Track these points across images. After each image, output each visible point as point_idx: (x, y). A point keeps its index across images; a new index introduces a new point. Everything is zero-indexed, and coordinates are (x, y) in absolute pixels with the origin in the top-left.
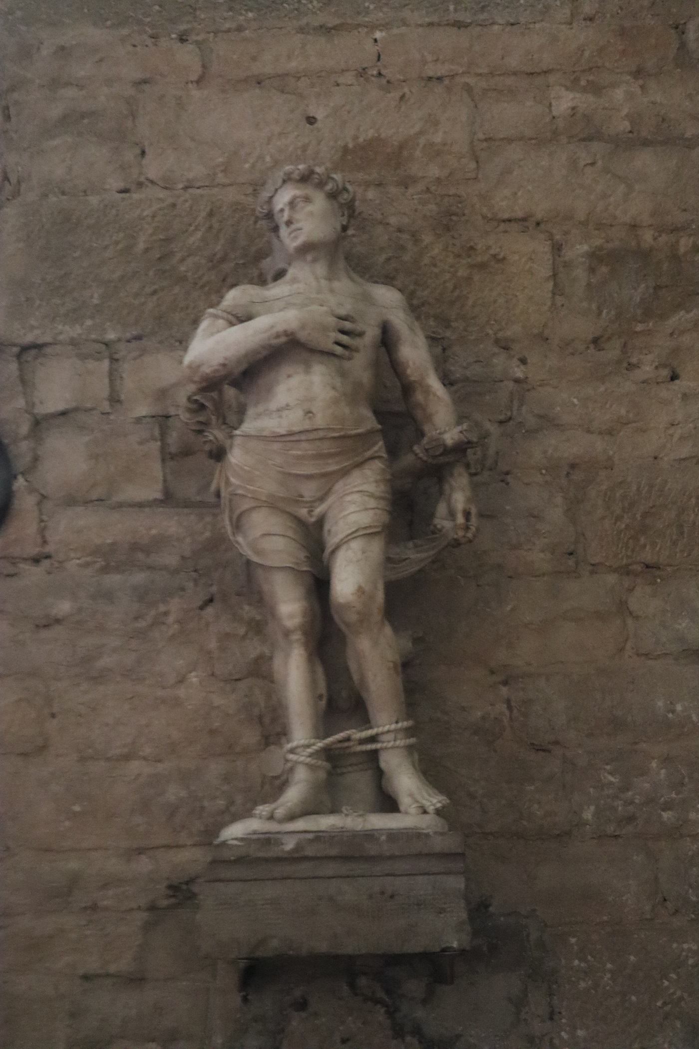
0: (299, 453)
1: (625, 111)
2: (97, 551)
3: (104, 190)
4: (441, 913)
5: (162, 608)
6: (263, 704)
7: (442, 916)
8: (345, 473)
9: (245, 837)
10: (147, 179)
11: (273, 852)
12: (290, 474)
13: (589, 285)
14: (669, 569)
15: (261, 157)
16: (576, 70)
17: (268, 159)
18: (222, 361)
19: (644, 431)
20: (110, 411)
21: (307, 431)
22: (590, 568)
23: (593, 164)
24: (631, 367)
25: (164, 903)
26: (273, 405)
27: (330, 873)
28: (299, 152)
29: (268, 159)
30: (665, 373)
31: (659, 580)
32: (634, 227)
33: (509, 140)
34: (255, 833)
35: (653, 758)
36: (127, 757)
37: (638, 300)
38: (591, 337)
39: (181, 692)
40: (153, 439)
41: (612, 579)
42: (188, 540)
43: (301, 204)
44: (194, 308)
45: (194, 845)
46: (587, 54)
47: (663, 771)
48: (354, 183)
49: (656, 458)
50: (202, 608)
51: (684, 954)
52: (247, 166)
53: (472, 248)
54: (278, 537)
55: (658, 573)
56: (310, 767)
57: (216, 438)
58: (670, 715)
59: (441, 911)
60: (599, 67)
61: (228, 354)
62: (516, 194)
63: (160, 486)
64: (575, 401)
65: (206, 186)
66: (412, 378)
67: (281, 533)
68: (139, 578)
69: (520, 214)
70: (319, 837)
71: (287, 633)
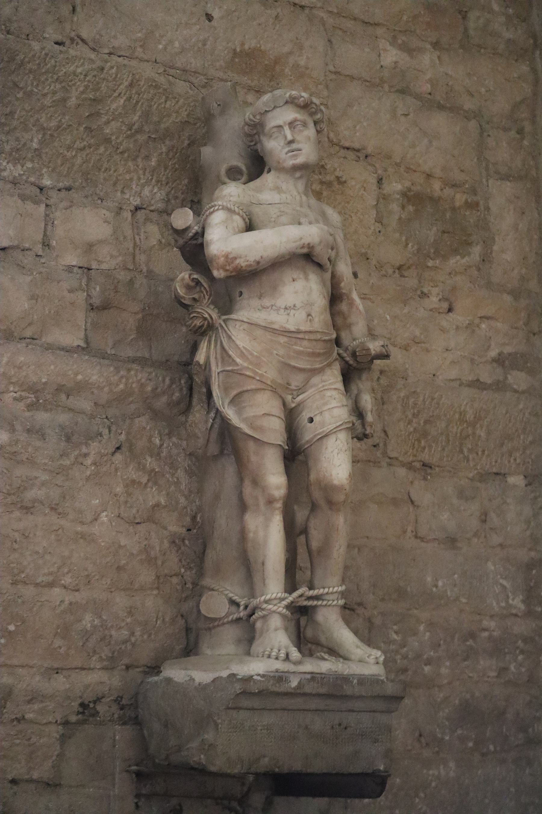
0: (301, 349)
1: (428, 76)
2: (33, 389)
3: (44, 38)
4: (375, 743)
5: (84, 450)
6: (158, 549)
7: (376, 745)
8: (320, 371)
9: (266, 673)
10: (79, 37)
11: (282, 688)
12: (289, 365)
13: (400, 219)
14: (437, 469)
15: (171, 42)
16: (396, 29)
17: (177, 44)
18: (258, 258)
19: (428, 351)
20: (41, 254)
21: (310, 332)
22: (388, 460)
23: (406, 115)
24: (424, 295)
25: (73, 718)
26: (281, 302)
27: (313, 706)
28: (200, 45)
29: (177, 44)
30: (445, 305)
31: (429, 477)
32: (429, 176)
33: (352, 78)
34: (277, 671)
35: (422, 623)
36: (51, 585)
37: (432, 241)
38: (398, 264)
39: (95, 529)
40: (80, 288)
41: (402, 472)
42: (106, 389)
43: (300, 127)
44: (115, 171)
45: (103, 668)
46: (405, 18)
47: (428, 634)
48: (240, 84)
49: (434, 375)
50: (113, 454)
51: (430, 778)
52: (160, 47)
53: (323, 166)
54: (276, 418)
55: (429, 471)
56: (283, 616)
57: (211, 318)
58: (434, 589)
59: (376, 741)
60: (411, 32)
61: (265, 255)
62: (355, 127)
63: (82, 334)
64: (388, 317)
65: (126, 57)
66: (344, 291)
67: (277, 415)
68: (63, 418)
69: (357, 145)
70: (314, 677)
71: (270, 502)
